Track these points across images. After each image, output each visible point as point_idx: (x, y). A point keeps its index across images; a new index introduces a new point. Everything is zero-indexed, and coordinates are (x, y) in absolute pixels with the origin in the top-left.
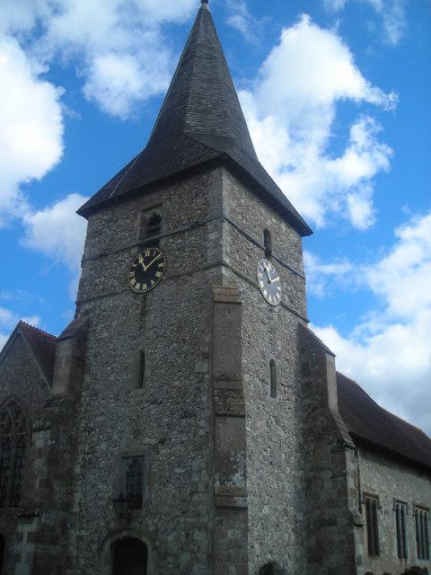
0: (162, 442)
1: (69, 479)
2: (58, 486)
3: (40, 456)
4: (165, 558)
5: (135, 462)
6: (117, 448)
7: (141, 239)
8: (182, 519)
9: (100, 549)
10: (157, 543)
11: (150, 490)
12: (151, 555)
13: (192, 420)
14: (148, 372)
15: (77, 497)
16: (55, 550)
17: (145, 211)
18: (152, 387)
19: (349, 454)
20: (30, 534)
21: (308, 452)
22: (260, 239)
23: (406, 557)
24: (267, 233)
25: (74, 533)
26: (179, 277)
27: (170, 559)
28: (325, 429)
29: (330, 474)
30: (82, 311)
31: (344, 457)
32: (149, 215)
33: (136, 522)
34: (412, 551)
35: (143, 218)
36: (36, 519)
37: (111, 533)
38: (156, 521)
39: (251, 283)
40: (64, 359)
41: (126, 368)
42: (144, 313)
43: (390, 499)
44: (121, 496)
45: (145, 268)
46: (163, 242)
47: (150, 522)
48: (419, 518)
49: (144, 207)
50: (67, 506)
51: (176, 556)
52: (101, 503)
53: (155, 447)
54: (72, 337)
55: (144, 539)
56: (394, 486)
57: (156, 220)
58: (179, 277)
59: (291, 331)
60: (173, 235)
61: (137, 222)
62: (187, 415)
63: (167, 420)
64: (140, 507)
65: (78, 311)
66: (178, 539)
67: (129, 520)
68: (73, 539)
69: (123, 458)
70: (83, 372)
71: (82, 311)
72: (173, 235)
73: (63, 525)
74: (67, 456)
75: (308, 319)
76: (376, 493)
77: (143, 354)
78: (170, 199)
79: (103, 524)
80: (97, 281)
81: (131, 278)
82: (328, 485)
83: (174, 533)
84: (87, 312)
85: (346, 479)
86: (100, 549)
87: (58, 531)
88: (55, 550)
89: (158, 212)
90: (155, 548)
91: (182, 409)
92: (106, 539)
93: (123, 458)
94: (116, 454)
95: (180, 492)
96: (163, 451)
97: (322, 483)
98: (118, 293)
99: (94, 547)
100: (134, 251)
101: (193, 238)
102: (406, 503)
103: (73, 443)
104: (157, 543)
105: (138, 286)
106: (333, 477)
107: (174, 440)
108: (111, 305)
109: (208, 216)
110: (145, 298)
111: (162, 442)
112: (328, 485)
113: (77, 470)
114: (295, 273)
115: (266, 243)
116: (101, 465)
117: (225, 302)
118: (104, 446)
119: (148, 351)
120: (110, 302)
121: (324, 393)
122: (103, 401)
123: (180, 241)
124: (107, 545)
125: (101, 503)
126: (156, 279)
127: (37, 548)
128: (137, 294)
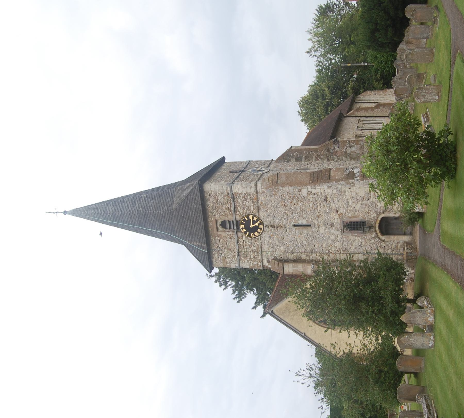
0: (337, 211)
5: (345, 226)
6: (339, 236)
7: (233, 232)
8: (371, 200)
9: (384, 241)
10: (381, 212)
11: (358, 217)
13: (328, 197)
14: (304, 222)
17: (217, 231)
18: (311, 219)
21: (338, 159)
22: (236, 175)
24: (231, 172)
26: (258, 207)
28: (328, 150)
29: (348, 148)
31: (341, 141)
32: (220, 228)
33: (372, 223)
34: (379, 125)
35: (221, 231)
37: (377, 236)
38: (372, 213)
40: (295, 269)
41: (301, 234)
42: (274, 227)
43: (357, 131)
45: (251, 226)
46: (238, 218)
47: (372, 216)
48: (364, 123)
52: (363, 244)
53: (339, 215)
54: (283, 264)
55: (380, 218)
58: (258, 207)
59: (280, 166)
60: (235, 212)
61: (223, 234)
62: (326, 199)
63: (328, 210)
64: (365, 222)
67: (371, 227)
69: (343, 232)
72: (235, 212)
75: (271, 159)
76: (354, 135)
77: (294, 226)
78: (214, 215)
79: (373, 241)
80: (252, 257)
81: (254, 235)
83: (377, 204)
85: (351, 141)
86: (384, 241)
89: (219, 222)
90: (383, 212)
91: (323, 202)
92: (379, 239)
93: (343, 232)
94: (341, 236)
95: (360, 201)
97: (352, 152)
98: (261, 243)
99: (383, 245)
100: (240, 234)
101: (239, 200)
102: (357, 127)
104: (381, 212)
105: (259, 231)
106: (350, 147)
107: (337, 206)
108: (267, 246)
109: (229, 192)
110: (267, 226)
112: (353, 149)
114: (248, 164)
115: (236, 172)
116: (346, 244)
118: (337, 244)
119: (293, 223)
120: (265, 247)
121: (311, 150)
122: (316, 246)
123: (239, 208)
124: (383, 238)
125: (363, 244)
128: (263, 231)
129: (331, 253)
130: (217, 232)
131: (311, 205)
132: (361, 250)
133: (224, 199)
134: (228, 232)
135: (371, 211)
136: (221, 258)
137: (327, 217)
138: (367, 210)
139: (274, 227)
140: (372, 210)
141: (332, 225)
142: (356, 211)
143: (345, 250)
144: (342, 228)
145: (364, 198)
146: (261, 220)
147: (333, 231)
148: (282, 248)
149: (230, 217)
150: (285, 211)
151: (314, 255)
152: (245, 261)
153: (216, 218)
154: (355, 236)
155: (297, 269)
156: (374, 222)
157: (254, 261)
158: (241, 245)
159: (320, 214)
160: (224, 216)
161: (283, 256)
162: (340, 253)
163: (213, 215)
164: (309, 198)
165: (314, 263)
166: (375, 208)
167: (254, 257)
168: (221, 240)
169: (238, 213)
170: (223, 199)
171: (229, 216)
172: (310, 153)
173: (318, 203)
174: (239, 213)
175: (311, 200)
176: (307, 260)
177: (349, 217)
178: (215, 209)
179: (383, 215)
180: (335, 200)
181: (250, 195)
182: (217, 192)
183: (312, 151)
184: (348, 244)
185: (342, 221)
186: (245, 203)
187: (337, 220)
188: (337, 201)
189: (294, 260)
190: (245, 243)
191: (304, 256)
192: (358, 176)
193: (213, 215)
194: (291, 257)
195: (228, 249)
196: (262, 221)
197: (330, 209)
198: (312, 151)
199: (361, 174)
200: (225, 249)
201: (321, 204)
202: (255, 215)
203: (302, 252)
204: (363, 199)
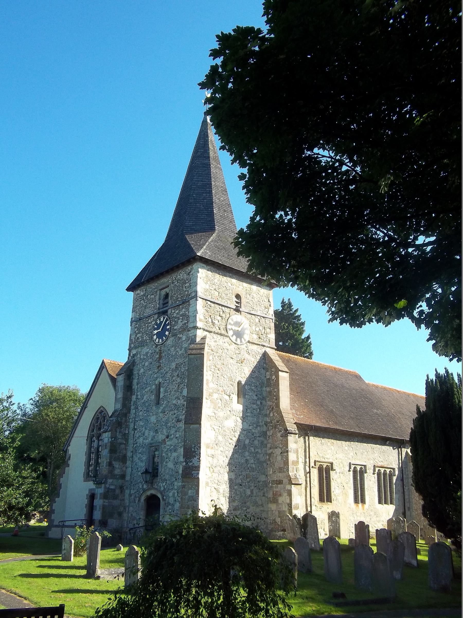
1: (124, 459)
2: (116, 465)
3: (106, 448)
4: (168, 506)
11: (162, 466)
12: (162, 503)
14: (162, 395)
15: (129, 470)
16: (116, 502)
19: (291, 439)
20: (101, 494)
23: (363, 501)
25: (127, 492)
27: (170, 507)
29: (280, 451)
30: (132, 355)
32: (163, 292)
35: (160, 294)
36: (103, 485)
38: (164, 484)
39: (221, 335)
41: (152, 392)
44: (146, 470)
46: (169, 312)
49: (161, 287)
50: (123, 477)
51: (173, 505)
56: (352, 454)
57: (167, 296)
65: (129, 355)
66: (174, 494)
68: (127, 496)
70: (131, 395)
71: (132, 355)
73: (121, 488)
74: (123, 446)
79: (141, 487)
80: (138, 335)
82: (279, 458)
84: (134, 355)
87: (118, 491)
88: (116, 502)
94: (147, 444)
96: (168, 443)
99: (137, 500)
100: (156, 316)
103: (126, 437)
111: (167, 437)
113: (129, 454)
116: (140, 451)
117: (194, 354)
118: (141, 439)
123: (178, 311)
126: (166, 336)
127: (104, 502)
129: (134, 432)
130: (160, 290)
131: (174, 402)
132: (134, 471)
133: (186, 291)
134: (159, 302)
135: (166, 483)
136: (139, 300)
137: (164, 424)
138: (167, 477)
139: (160, 358)
140: (167, 484)
141: (156, 431)
142: (166, 462)
143: (134, 452)
144: (153, 445)
145: (177, 474)
146: (166, 340)
147: (152, 433)
148: (142, 370)
149: (170, 302)
150: (171, 369)
151: (134, 411)
152: (135, 328)
153: (170, 286)
154: (145, 463)
155: (119, 391)
156: (156, 487)
157: (135, 338)
158: (148, 320)
159: (166, 415)
160: (171, 295)
161: (135, 372)
162: (134, 444)
163: (173, 281)
164: (181, 398)
165: (124, 411)
166: (169, 489)
167: (138, 338)
168: (153, 296)
169: (173, 311)
170: (185, 289)
171: (171, 301)
172: (275, 398)
173: (176, 412)
174: (173, 313)
175: (179, 401)
176: (130, 403)
177: (162, 454)
178: (178, 282)
179: (161, 500)
180: (177, 433)
181: (187, 323)
182: (192, 281)
183: (277, 400)
184: (140, 453)
185: (158, 444)
186: (180, 318)
187: (161, 437)
188: (177, 436)
189: (132, 387)
190: (149, 325)
191: (134, 397)
192: (187, 464)
193: (173, 281)
194: (135, 381)
195: (146, 306)
196: (165, 342)
197: (170, 427)
198: (277, 400)
199: (189, 467)
200: (146, 302)
201: (175, 416)
202: (170, 332)
203: (137, 395)
204: (177, 472)
